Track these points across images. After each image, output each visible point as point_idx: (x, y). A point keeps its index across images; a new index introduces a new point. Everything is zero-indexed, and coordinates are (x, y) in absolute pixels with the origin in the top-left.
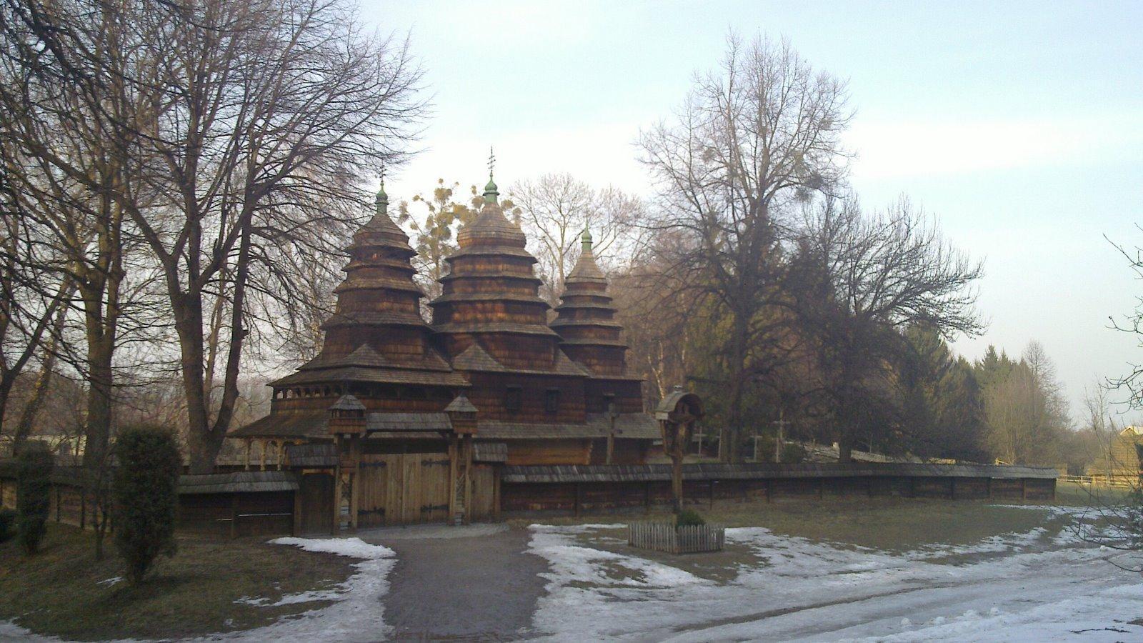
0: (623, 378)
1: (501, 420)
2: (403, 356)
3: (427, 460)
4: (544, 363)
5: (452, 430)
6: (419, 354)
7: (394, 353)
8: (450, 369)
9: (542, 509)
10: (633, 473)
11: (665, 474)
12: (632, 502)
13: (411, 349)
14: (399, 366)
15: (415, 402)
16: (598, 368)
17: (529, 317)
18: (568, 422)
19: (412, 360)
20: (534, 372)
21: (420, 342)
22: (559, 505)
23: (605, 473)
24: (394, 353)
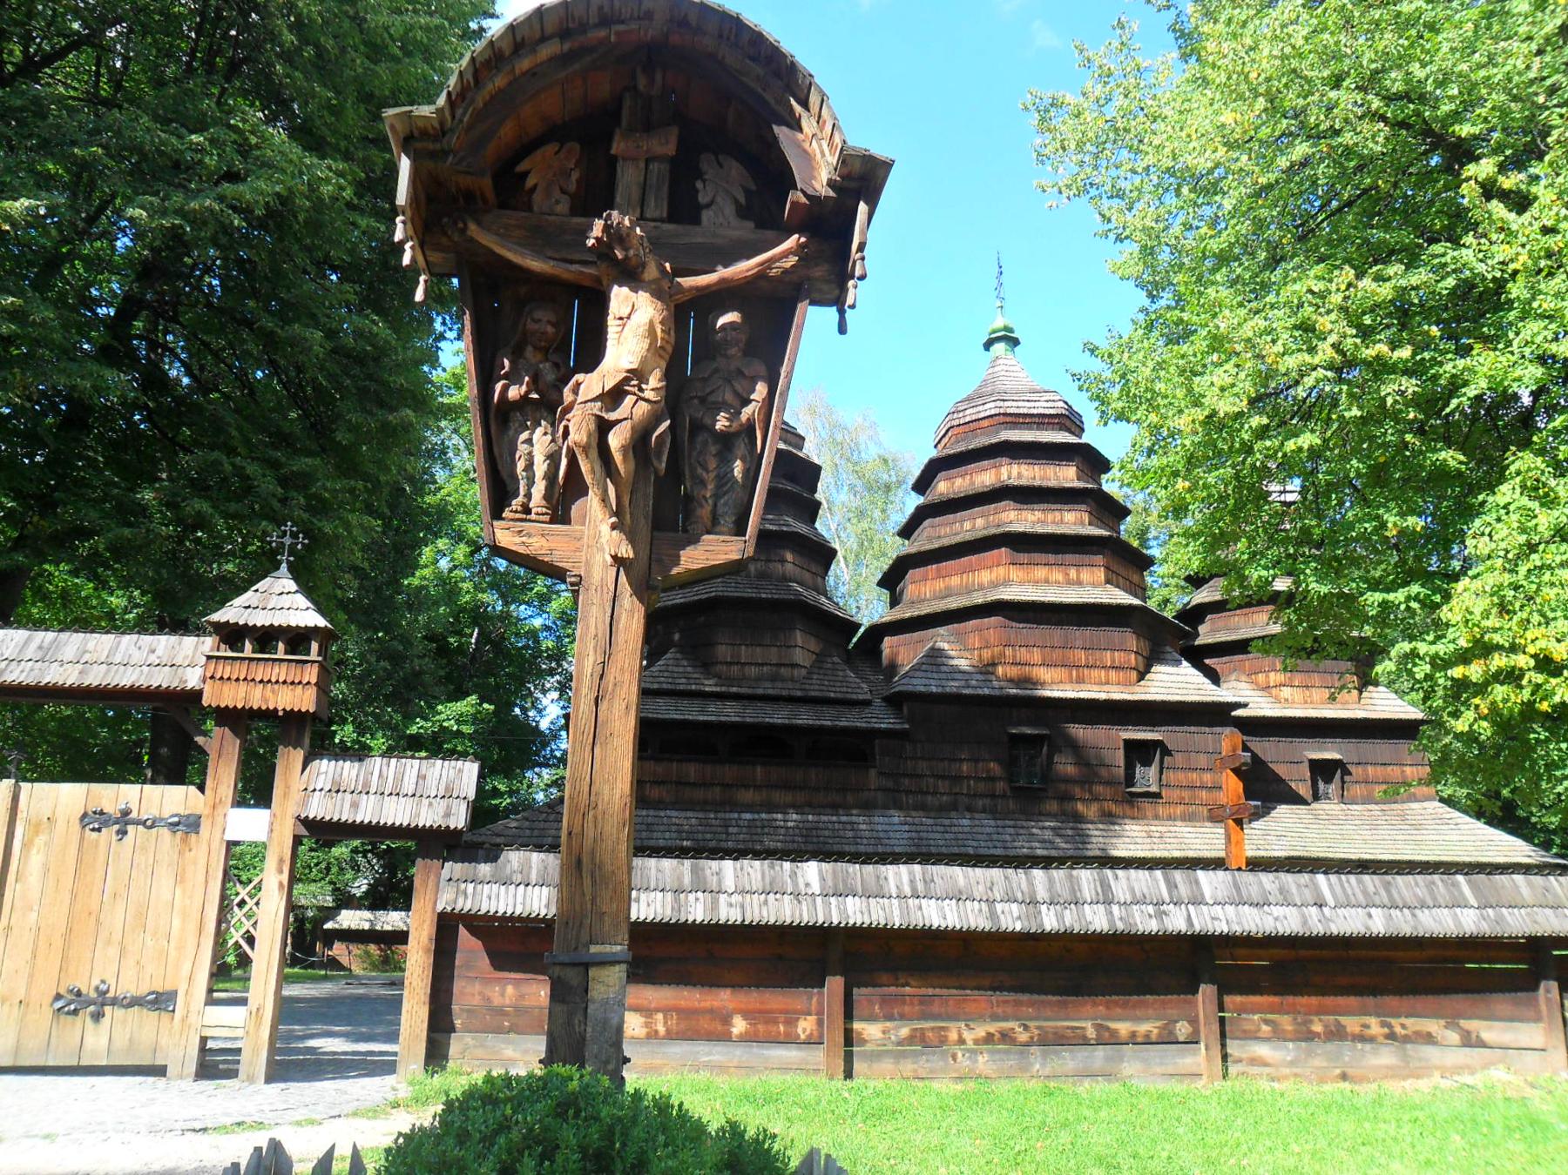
0: (1360, 714)
1: (994, 813)
2: (753, 671)
3: (111, 808)
4: (1113, 674)
5: (197, 695)
6: (797, 665)
7: (731, 663)
8: (868, 697)
9: (652, 1035)
10: (1108, 900)
11: (1277, 911)
12: (1123, 1028)
13: (773, 655)
14: (734, 689)
15: (759, 769)
16: (1286, 692)
17: (1073, 573)
18: (1188, 818)
19: (774, 678)
20: (1083, 695)
21: (799, 637)
22: (739, 1026)
23: (958, 897)
24: (731, 663)
